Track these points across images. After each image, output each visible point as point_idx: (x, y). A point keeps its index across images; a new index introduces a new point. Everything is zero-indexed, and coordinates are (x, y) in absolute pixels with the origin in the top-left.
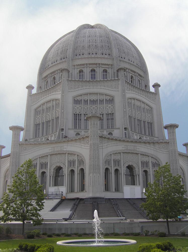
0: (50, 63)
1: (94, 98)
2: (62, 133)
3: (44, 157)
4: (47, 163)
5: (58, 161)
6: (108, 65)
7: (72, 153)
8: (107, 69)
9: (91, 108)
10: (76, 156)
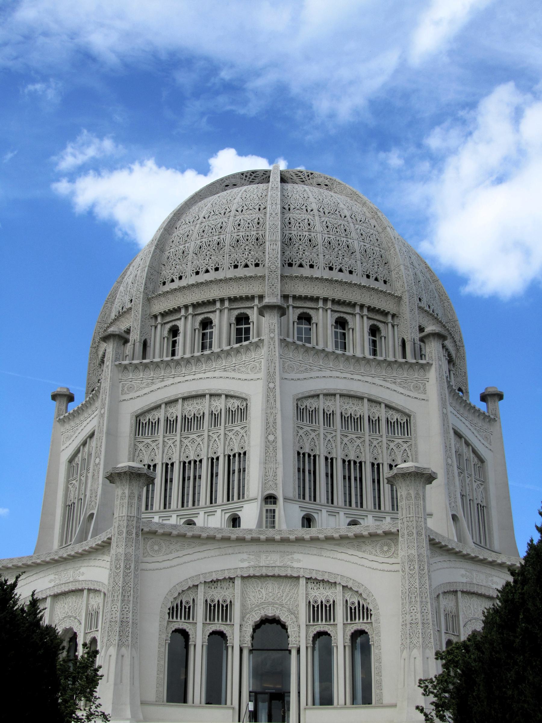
0: (189, 269)
1: (353, 408)
2: (267, 510)
3: (219, 583)
4: (231, 602)
5: (270, 600)
6: (385, 314)
7: (326, 578)
8: (381, 326)
9: (346, 440)
10: (339, 589)
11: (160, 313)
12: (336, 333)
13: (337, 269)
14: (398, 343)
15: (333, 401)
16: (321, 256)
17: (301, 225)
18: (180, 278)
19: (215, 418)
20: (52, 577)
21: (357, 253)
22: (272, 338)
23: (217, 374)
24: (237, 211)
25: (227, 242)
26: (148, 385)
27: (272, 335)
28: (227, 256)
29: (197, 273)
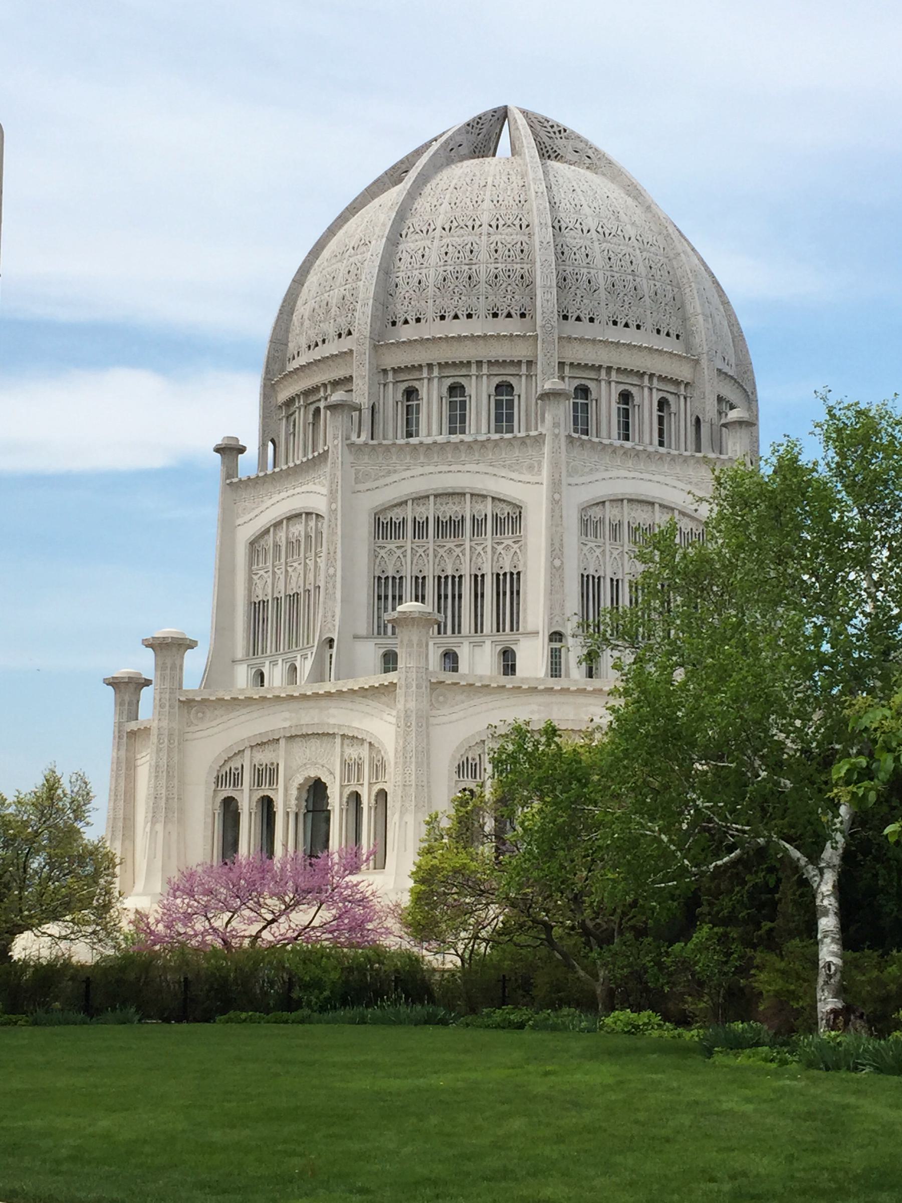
2: (552, 649)
6: (677, 383)
8: (671, 398)
11: (393, 369)
12: (619, 408)
13: (623, 323)
14: (691, 422)
15: (620, 508)
16: (603, 304)
17: (577, 256)
18: (418, 320)
19: (478, 524)
20: (286, 715)
21: (647, 297)
22: (557, 436)
23: (482, 467)
24: (490, 226)
25: (483, 277)
26: (389, 472)
27: (557, 431)
28: (482, 298)
29: (443, 318)
